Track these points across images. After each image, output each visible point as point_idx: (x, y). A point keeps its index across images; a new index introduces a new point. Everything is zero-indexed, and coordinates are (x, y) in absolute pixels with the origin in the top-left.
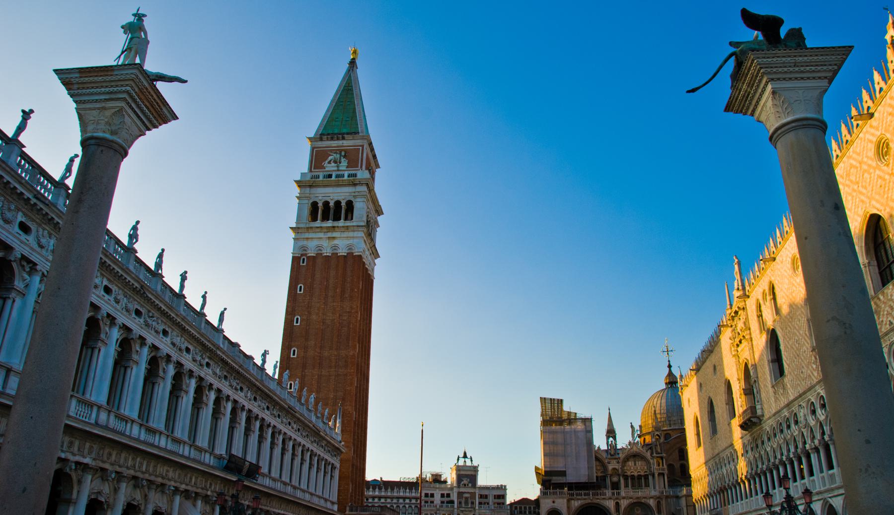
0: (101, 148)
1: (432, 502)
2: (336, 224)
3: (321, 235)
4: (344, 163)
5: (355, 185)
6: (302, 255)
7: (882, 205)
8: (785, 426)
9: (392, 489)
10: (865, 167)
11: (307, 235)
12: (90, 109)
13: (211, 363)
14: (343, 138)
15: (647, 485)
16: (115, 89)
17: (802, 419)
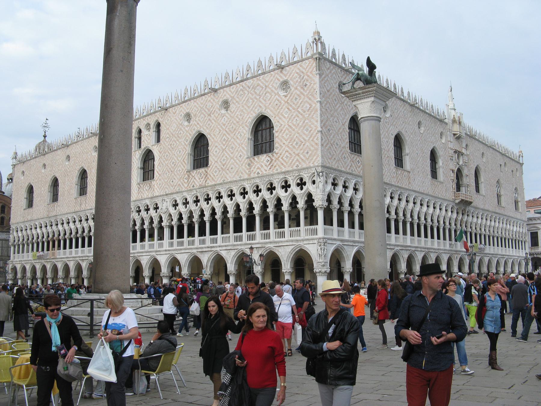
7: (274, 114)
10: (269, 91)
17: (164, 208)
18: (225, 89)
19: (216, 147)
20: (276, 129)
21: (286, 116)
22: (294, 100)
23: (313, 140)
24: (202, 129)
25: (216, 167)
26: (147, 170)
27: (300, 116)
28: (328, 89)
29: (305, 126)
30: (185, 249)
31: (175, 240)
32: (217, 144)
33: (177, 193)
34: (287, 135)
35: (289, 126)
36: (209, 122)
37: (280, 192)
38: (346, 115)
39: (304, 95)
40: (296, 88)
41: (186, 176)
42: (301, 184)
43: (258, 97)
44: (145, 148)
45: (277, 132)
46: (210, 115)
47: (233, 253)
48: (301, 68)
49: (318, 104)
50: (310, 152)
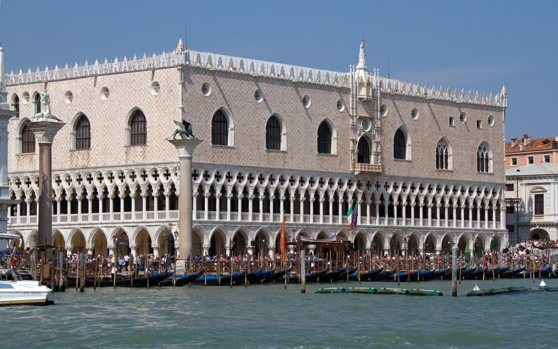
18: (105, 76)
19: (97, 131)
21: (156, 114)
24: (83, 111)
25: (97, 150)
26: (27, 141)
32: (98, 129)
34: (156, 131)
36: (90, 106)
37: (151, 179)
38: (209, 112)
40: (164, 92)
41: (69, 155)
42: (167, 175)
43: (134, 92)
44: (24, 119)
45: (149, 127)
46: (90, 99)
47: (112, 229)
49: (181, 110)
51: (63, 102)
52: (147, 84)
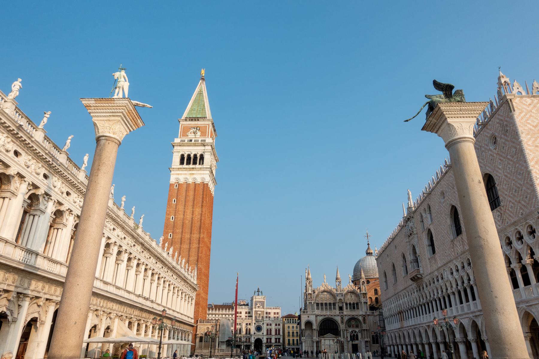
0: (108, 142)
1: (241, 317)
2: (194, 166)
3: (186, 172)
4: (199, 133)
5: (204, 146)
6: (175, 183)
8: (435, 280)
9: (219, 310)
10: (483, 149)
11: (178, 172)
12: (101, 120)
13: (136, 245)
14: (198, 120)
15: (358, 308)
16: (116, 111)
20: (497, 182)
21: (500, 167)
22: (502, 150)
23: (527, 183)
27: (511, 163)
28: (535, 124)
29: (517, 171)
30: (466, 314)
31: (459, 306)
33: (450, 262)
34: (506, 185)
35: (506, 176)
39: (508, 141)
40: (501, 138)
48: (500, 117)
50: (528, 196)
51: (440, 202)
52: (486, 143)
